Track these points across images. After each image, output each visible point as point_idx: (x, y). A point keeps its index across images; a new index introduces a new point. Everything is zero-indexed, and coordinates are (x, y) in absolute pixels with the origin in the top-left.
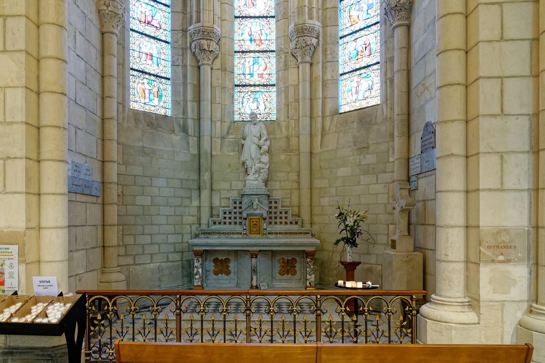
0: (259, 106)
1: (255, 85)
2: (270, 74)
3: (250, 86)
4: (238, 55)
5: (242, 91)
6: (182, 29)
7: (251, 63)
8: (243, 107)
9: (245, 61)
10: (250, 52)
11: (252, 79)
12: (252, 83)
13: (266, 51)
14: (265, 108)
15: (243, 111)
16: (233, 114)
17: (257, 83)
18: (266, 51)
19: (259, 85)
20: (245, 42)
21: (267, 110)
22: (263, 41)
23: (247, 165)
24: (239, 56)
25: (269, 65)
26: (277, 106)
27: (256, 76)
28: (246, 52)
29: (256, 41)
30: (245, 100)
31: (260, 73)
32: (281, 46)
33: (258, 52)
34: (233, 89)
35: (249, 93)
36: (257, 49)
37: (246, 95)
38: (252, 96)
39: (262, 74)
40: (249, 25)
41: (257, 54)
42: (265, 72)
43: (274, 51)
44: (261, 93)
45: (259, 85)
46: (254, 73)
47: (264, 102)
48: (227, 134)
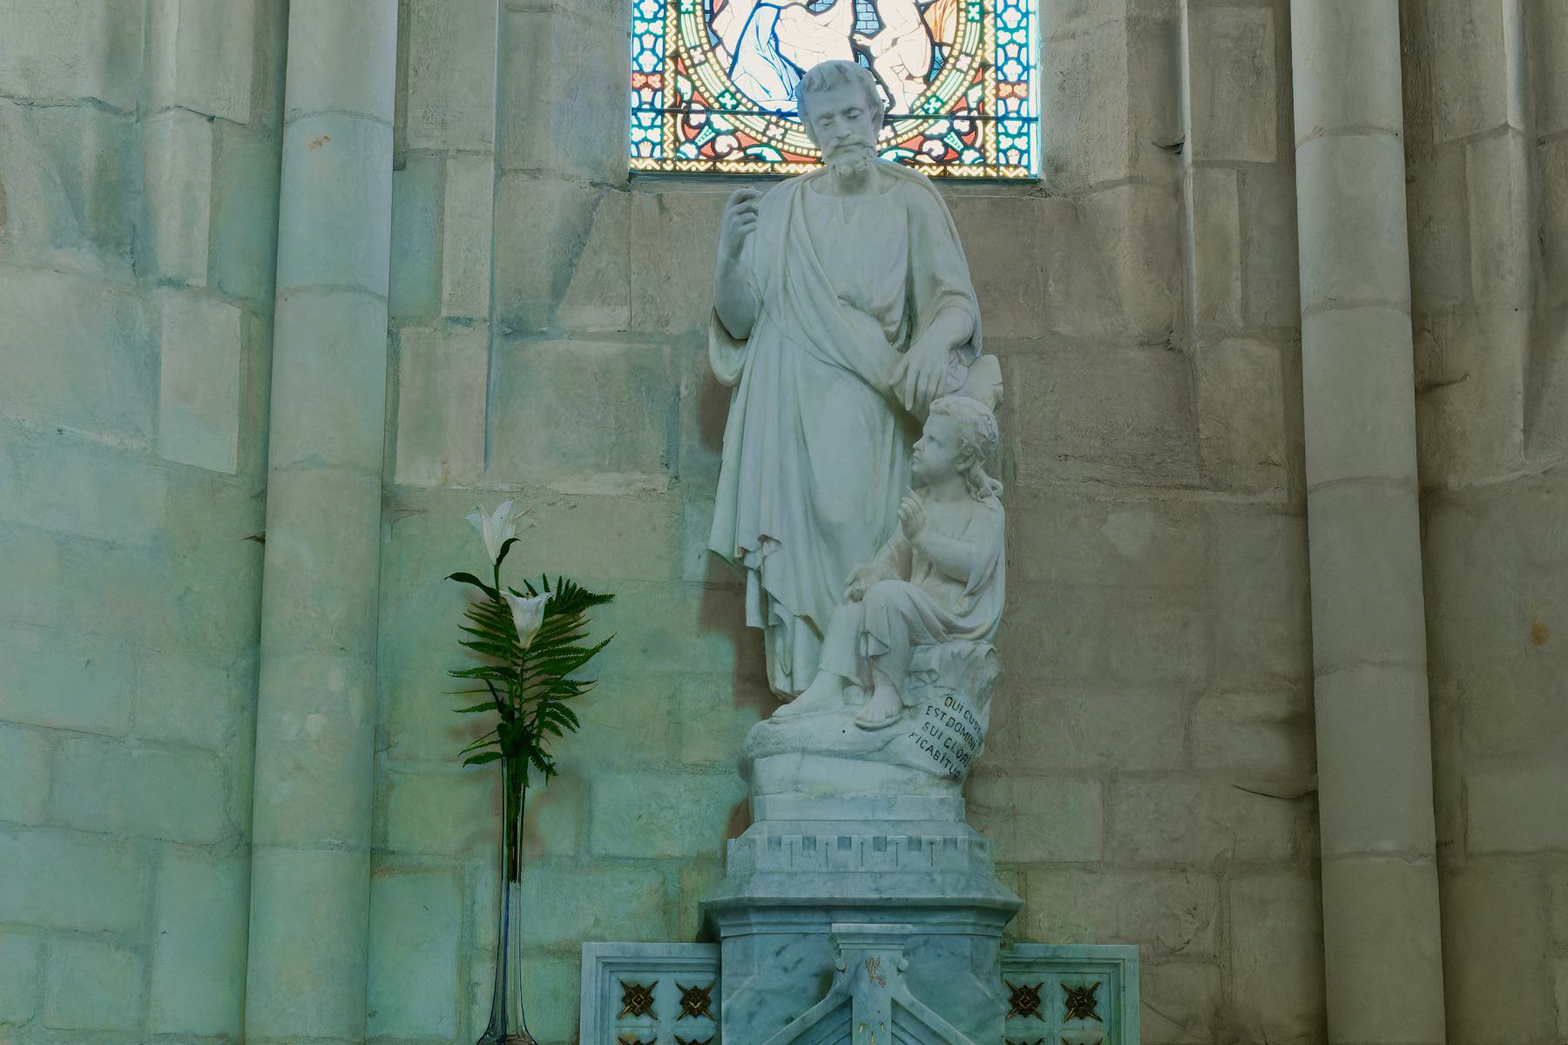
0: (875, 46)
23: (766, 599)
26: (1050, 40)
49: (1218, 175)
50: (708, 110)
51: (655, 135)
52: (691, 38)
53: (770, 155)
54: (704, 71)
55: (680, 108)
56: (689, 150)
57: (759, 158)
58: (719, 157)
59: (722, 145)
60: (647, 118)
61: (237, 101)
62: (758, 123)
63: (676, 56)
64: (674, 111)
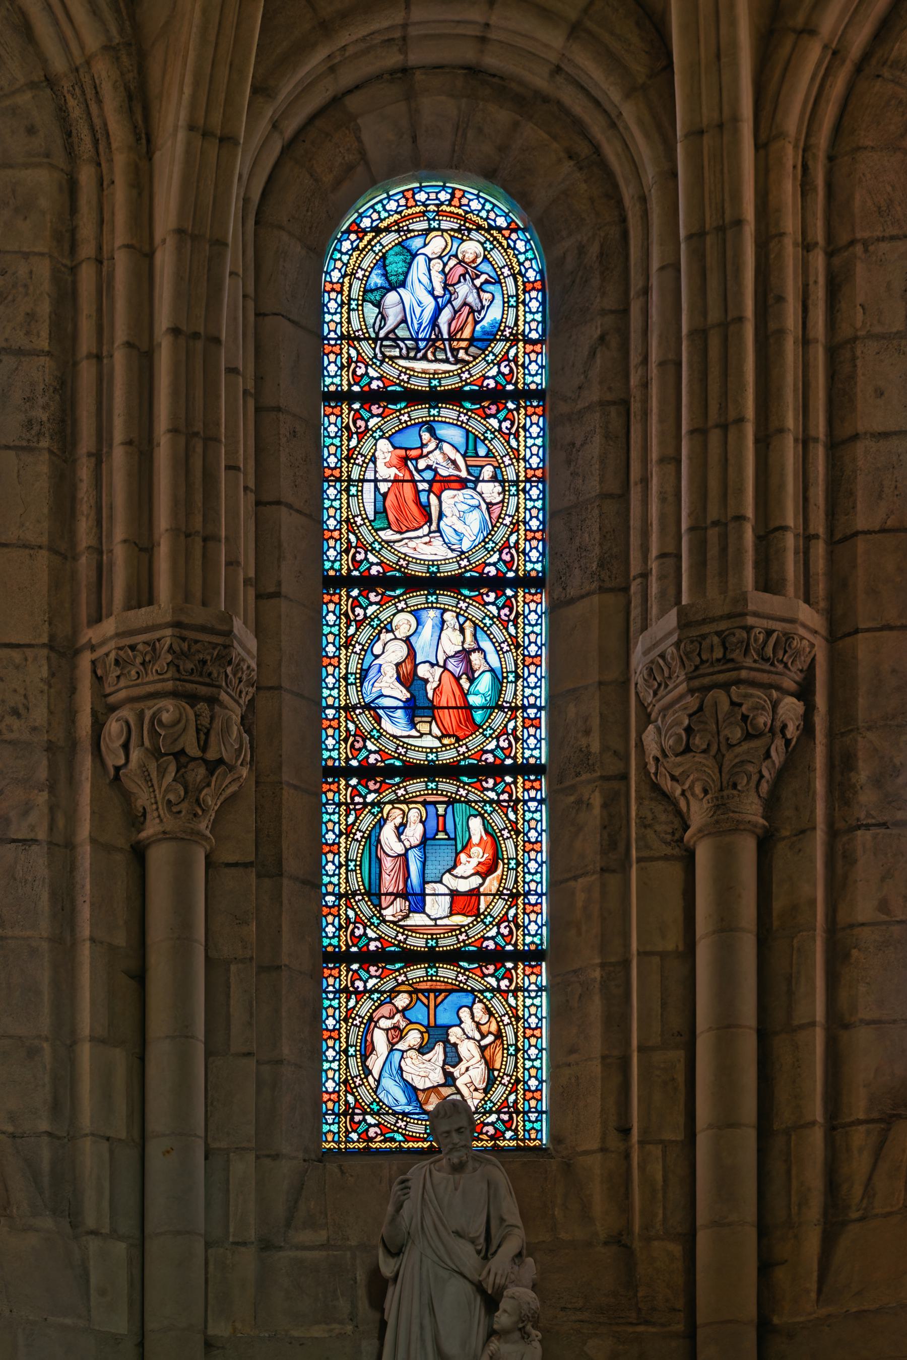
1: (432, 957)
2: (515, 896)
3: (410, 957)
4: (343, 790)
5: (359, 984)
6: (52, 637)
7: (414, 833)
8: (368, 1072)
9: (381, 823)
10: (411, 771)
11: (417, 919)
12: (417, 943)
13: (497, 771)
14: (491, 1082)
15: (365, 1095)
16: (319, 1117)
17: (447, 943)
18: (497, 771)
19: (453, 957)
20: (378, 719)
21: (498, 1093)
22: (478, 716)
24: (345, 795)
25: (510, 844)
27: (437, 906)
28: (389, 772)
29: (445, 715)
30: (380, 1039)
31: (463, 886)
32: (583, 742)
33: (451, 771)
34: (318, 978)
35: (402, 1001)
36: (447, 756)
37: (386, 1010)
38: (419, 1013)
39: (475, 893)
40: (404, 623)
41: (447, 786)
42: (492, 884)
43: (538, 769)
44: (468, 1000)
45: (453, 957)
46: (429, 889)
47: (483, 1049)
48: (288, 1224)
49: (650, 1147)
50: (365, 1113)
51: (334, 1128)
52: (354, 1072)
53: (399, 1137)
54: (362, 1090)
55: (348, 1112)
56: (354, 1136)
57: (392, 1140)
58: (371, 1140)
59: (372, 1132)
60: (330, 1119)
61: (120, 1129)
62: (392, 1119)
63: (346, 1082)
64: (345, 1114)
